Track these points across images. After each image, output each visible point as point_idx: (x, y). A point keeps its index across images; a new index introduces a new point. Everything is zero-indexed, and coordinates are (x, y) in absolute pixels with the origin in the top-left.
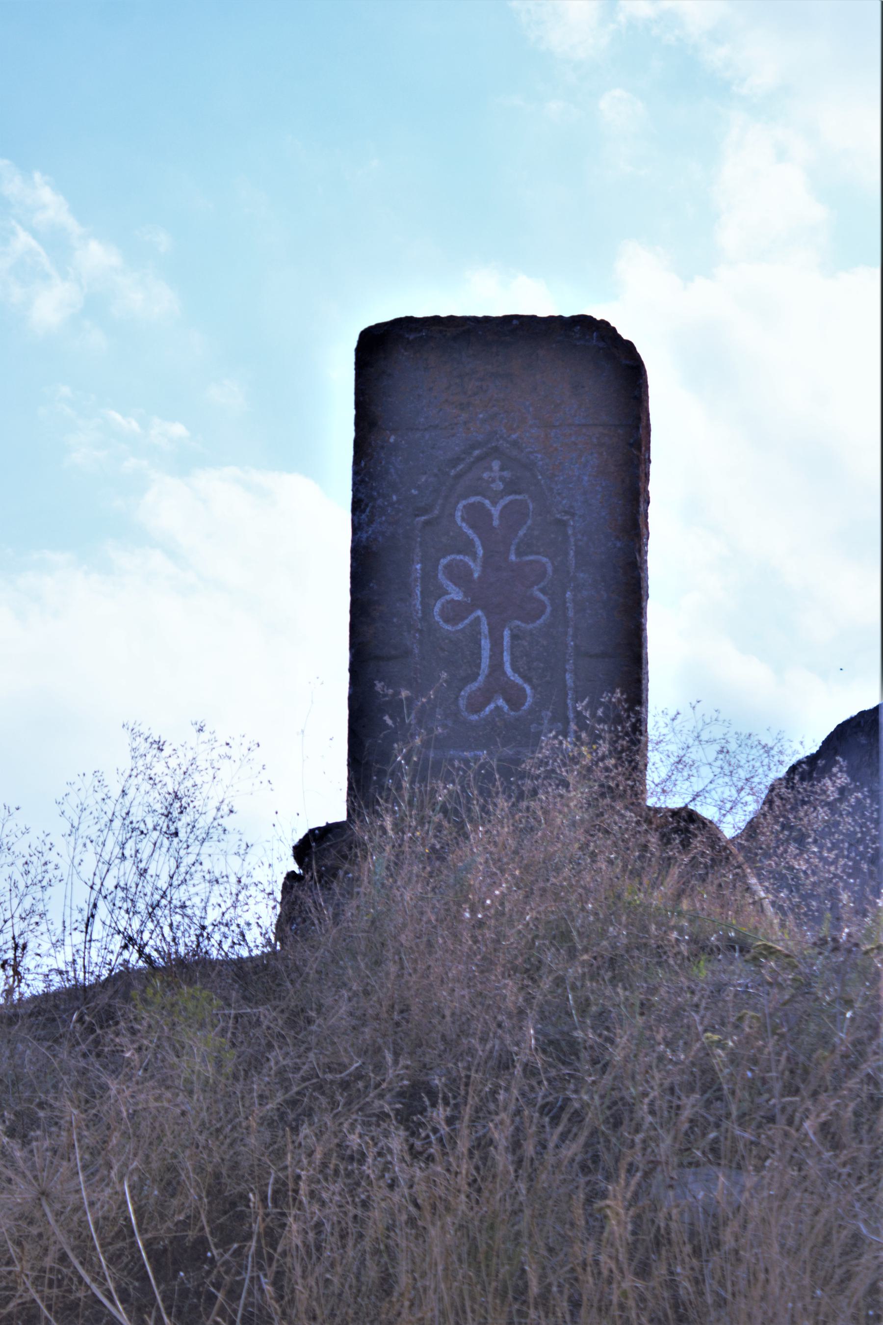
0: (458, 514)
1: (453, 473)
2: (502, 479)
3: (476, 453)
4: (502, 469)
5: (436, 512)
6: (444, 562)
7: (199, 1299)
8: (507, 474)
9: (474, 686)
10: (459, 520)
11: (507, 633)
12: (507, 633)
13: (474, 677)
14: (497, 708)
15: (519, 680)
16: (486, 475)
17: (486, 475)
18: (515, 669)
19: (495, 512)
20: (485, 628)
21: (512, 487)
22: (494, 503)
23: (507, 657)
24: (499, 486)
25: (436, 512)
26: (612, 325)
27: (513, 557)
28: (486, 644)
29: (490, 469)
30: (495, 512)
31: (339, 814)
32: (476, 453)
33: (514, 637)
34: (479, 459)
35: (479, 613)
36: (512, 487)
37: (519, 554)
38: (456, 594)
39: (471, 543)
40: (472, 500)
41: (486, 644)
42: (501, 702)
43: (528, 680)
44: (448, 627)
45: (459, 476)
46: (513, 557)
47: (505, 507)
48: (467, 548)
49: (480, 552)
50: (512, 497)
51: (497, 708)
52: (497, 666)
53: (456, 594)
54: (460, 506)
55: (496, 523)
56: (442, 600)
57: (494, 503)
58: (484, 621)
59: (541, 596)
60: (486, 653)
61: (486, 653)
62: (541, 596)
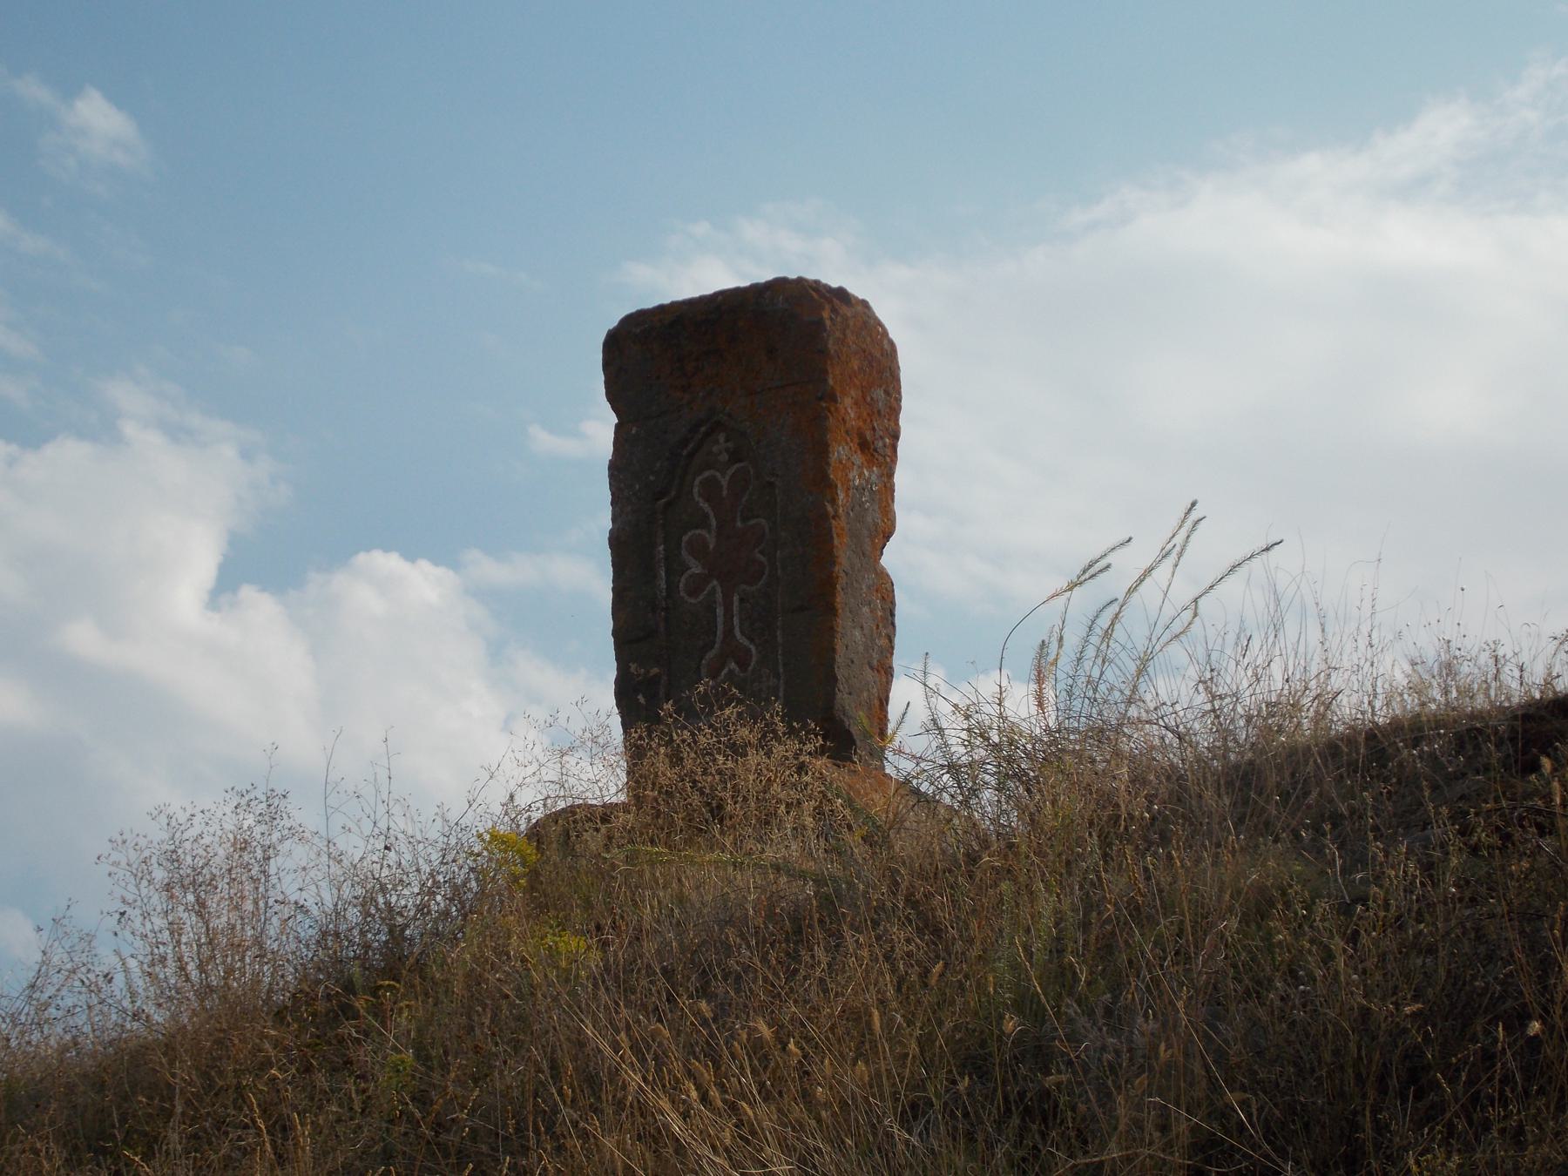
0: (696, 490)
1: (685, 453)
2: (727, 450)
3: (703, 429)
4: (727, 441)
5: (673, 493)
6: (685, 538)
7: (1450, 1120)
8: (730, 445)
9: (711, 654)
10: (696, 496)
11: (736, 598)
12: (736, 598)
13: (711, 646)
14: (731, 671)
15: (746, 642)
16: (715, 449)
17: (715, 449)
18: (742, 633)
19: (724, 482)
20: (719, 596)
21: (735, 456)
22: (723, 475)
23: (736, 621)
24: (724, 457)
25: (673, 493)
26: (793, 276)
27: (739, 524)
28: (720, 611)
29: (717, 442)
30: (724, 482)
31: (602, 779)
32: (703, 429)
33: (742, 600)
34: (707, 435)
35: (715, 582)
36: (735, 456)
37: (745, 519)
38: (696, 568)
39: (706, 516)
40: (707, 474)
41: (720, 611)
42: (733, 665)
43: (752, 640)
44: (693, 601)
45: (691, 455)
46: (739, 524)
47: (733, 475)
48: (703, 522)
49: (714, 523)
50: (737, 466)
51: (731, 671)
52: (729, 632)
53: (696, 568)
54: (697, 482)
55: (725, 493)
56: (686, 575)
57: (723, 475)
58: (719, 589)
59: (762, 558)
60: (720, 620)
61: (720, 620)
62: (762, 558)
